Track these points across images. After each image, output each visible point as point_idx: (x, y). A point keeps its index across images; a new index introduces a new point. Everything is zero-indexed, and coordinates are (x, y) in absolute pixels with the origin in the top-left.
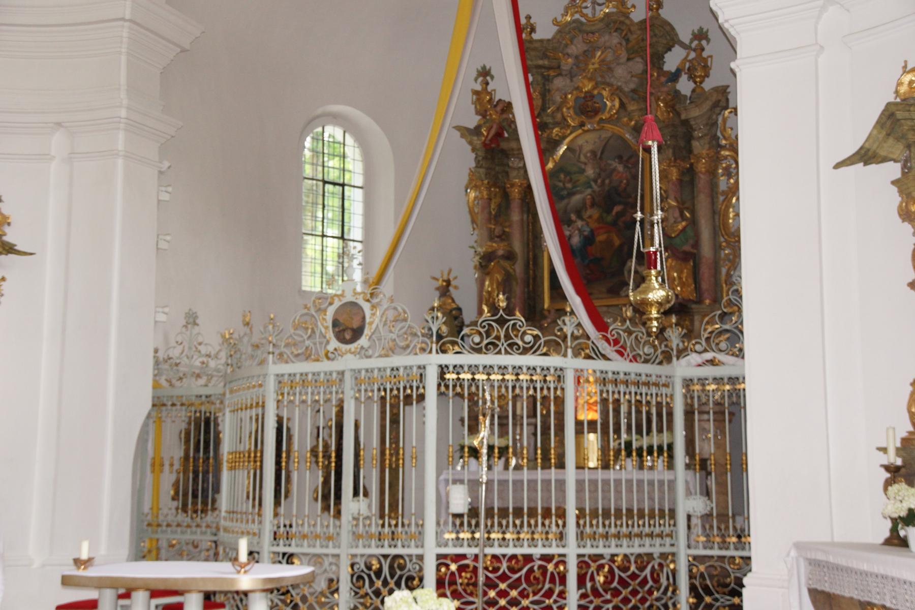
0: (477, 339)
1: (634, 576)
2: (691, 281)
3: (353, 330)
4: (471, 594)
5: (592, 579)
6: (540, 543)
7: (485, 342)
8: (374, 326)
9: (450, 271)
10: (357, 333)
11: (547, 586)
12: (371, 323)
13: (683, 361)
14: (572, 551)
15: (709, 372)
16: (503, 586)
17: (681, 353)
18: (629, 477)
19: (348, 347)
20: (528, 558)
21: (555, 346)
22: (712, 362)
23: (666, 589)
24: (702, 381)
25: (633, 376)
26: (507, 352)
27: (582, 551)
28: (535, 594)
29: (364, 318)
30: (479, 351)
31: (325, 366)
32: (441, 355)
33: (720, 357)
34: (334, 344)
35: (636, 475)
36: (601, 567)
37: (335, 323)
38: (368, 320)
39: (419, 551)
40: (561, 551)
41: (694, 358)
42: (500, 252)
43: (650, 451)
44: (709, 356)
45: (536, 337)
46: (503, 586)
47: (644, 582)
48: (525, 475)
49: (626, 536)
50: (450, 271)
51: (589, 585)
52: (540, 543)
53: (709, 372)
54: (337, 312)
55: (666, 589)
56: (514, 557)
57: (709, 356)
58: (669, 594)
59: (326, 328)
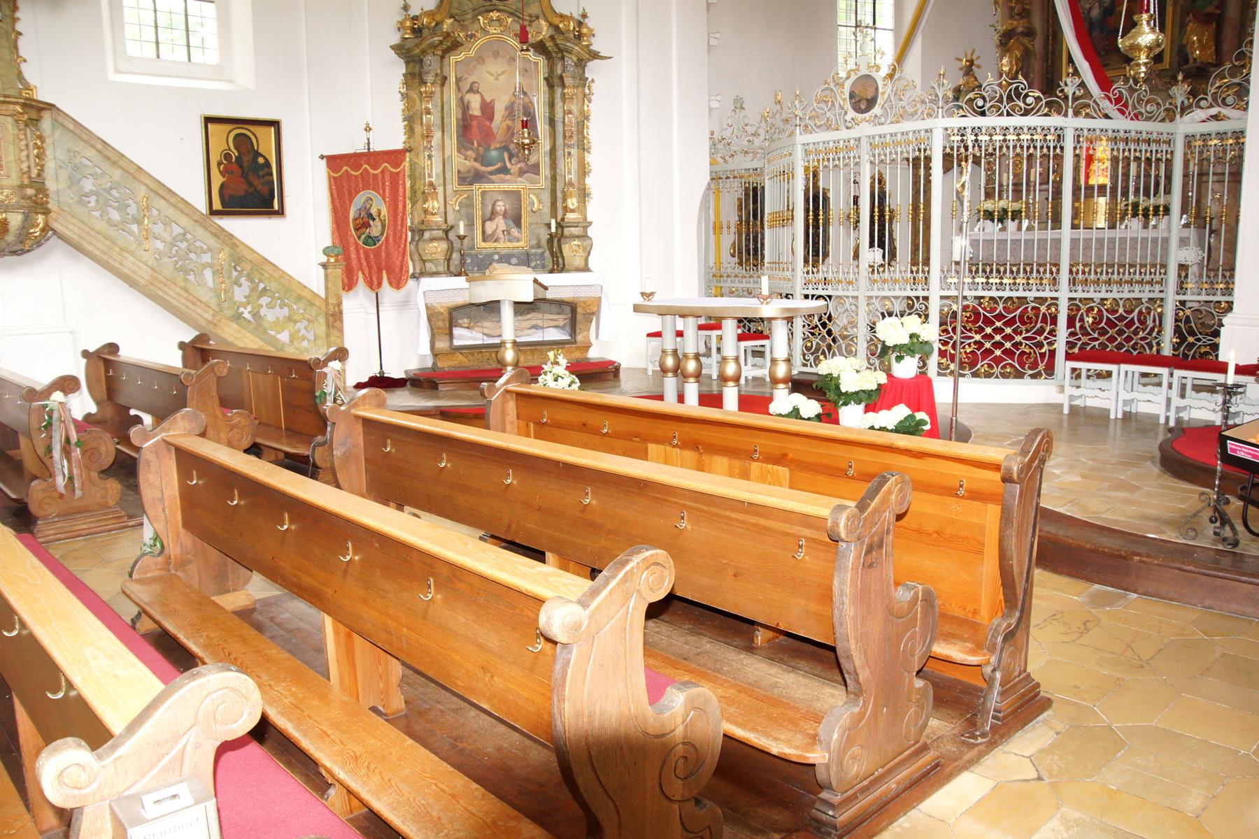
0: (980, 103)
1: (1121, 318)
2: (1212, 44)
3: (867, 100)
4: (970, 330)
5: (1082, 320)
6: (1034, 288)
7: (988, 105)
8: (886, 96)
9: (973, 52)
10: (871, 103)
11: (1039, 325)
12: (883, 94)
13: (1187, 118)
14: (1064, 294)
15: (1213, 127)
16: (998, 324)
17: (1184, 110)
18: (1134, 235)
19: (863, 116)
20: (1023, 300)
21: (1055, 107)
22: (1216, 117)
23: (1152, 329)
24: (1205, 137)
25: (1133, 133)
26: (1009, 114)
27: (1073, 295)
28: (1027, 331)
29: (877, 89)
30: (983, 114)
31: (843, 134)
32: (947, 119)
33: (1225, 111)
34: (851, 114)
35: (1142, 234)
36: (1091, 309)
37: (852, 96)
38: (880, 90)
39: (925, 294)
40: (1054, 295)
41: (1199, 114)
42: (1020, 29)
43: (1156, 213)
44: (1213, 111)
45: (1038, 99)
46: (998, 324)
47: (1132, 322)
48: (1037, 235)
49: (1116, 282)
50: (973, 52)
51: (1078, 325)
52: (1034, 288)
53: (1213, 127)
54: (853, 85)
55: (1152, 329)
56: (1010, 298)
57: (1213, 111)
58: (1154, 334)
59: (844, 100)
